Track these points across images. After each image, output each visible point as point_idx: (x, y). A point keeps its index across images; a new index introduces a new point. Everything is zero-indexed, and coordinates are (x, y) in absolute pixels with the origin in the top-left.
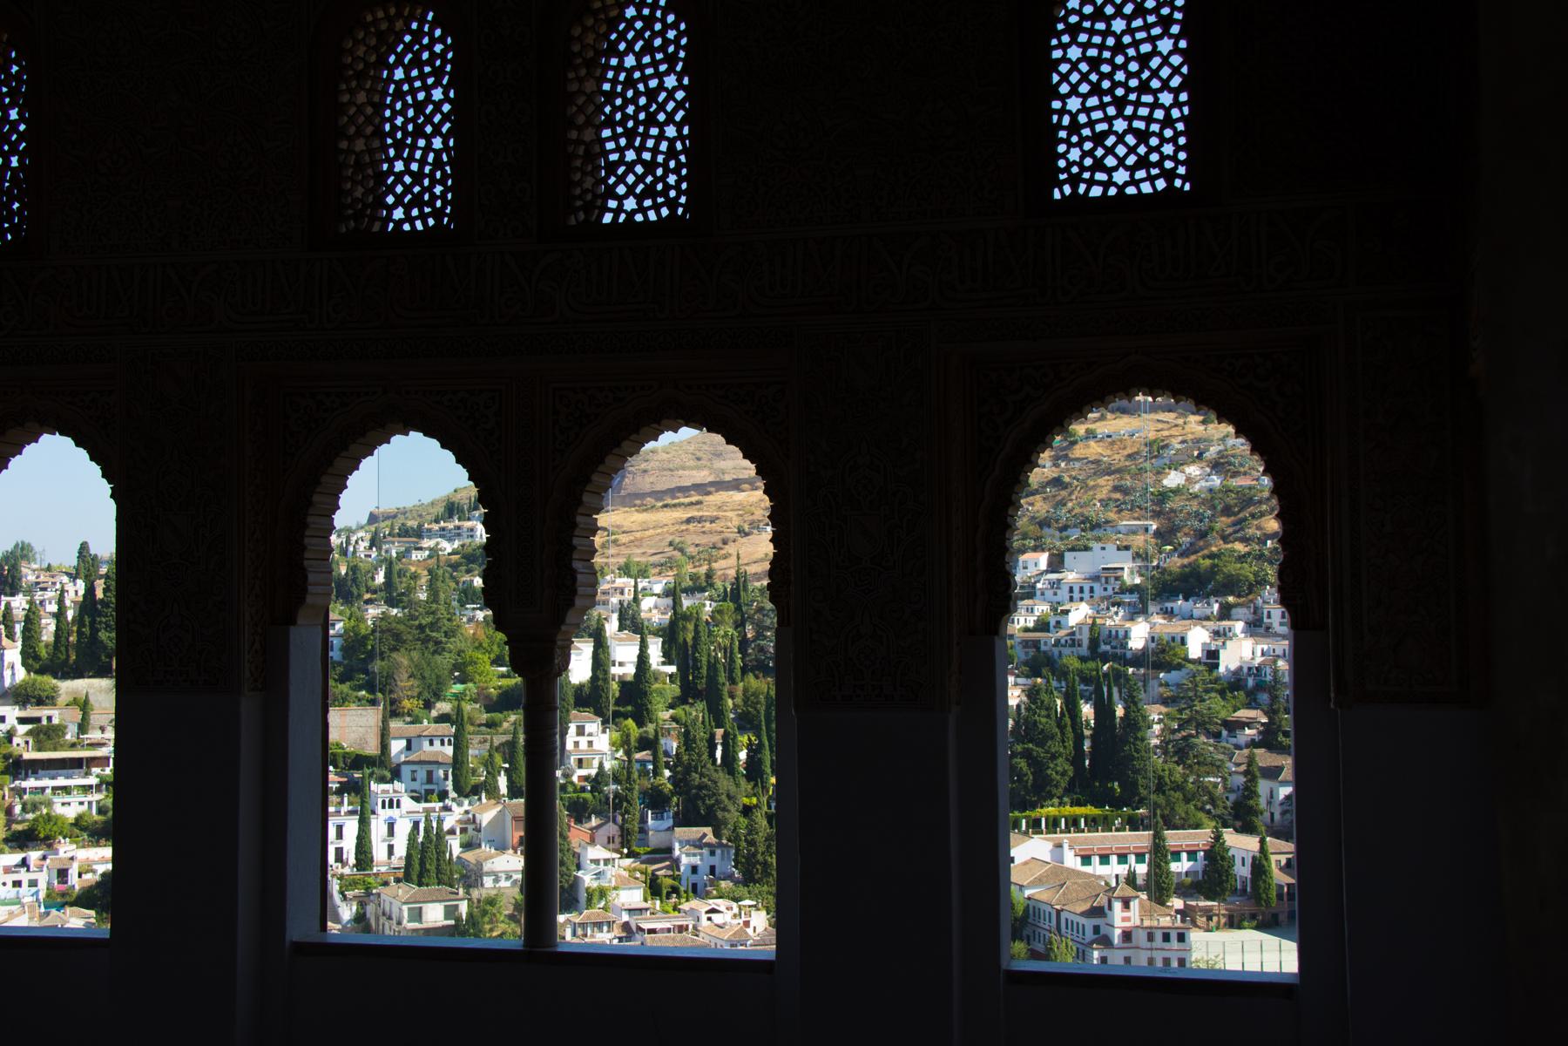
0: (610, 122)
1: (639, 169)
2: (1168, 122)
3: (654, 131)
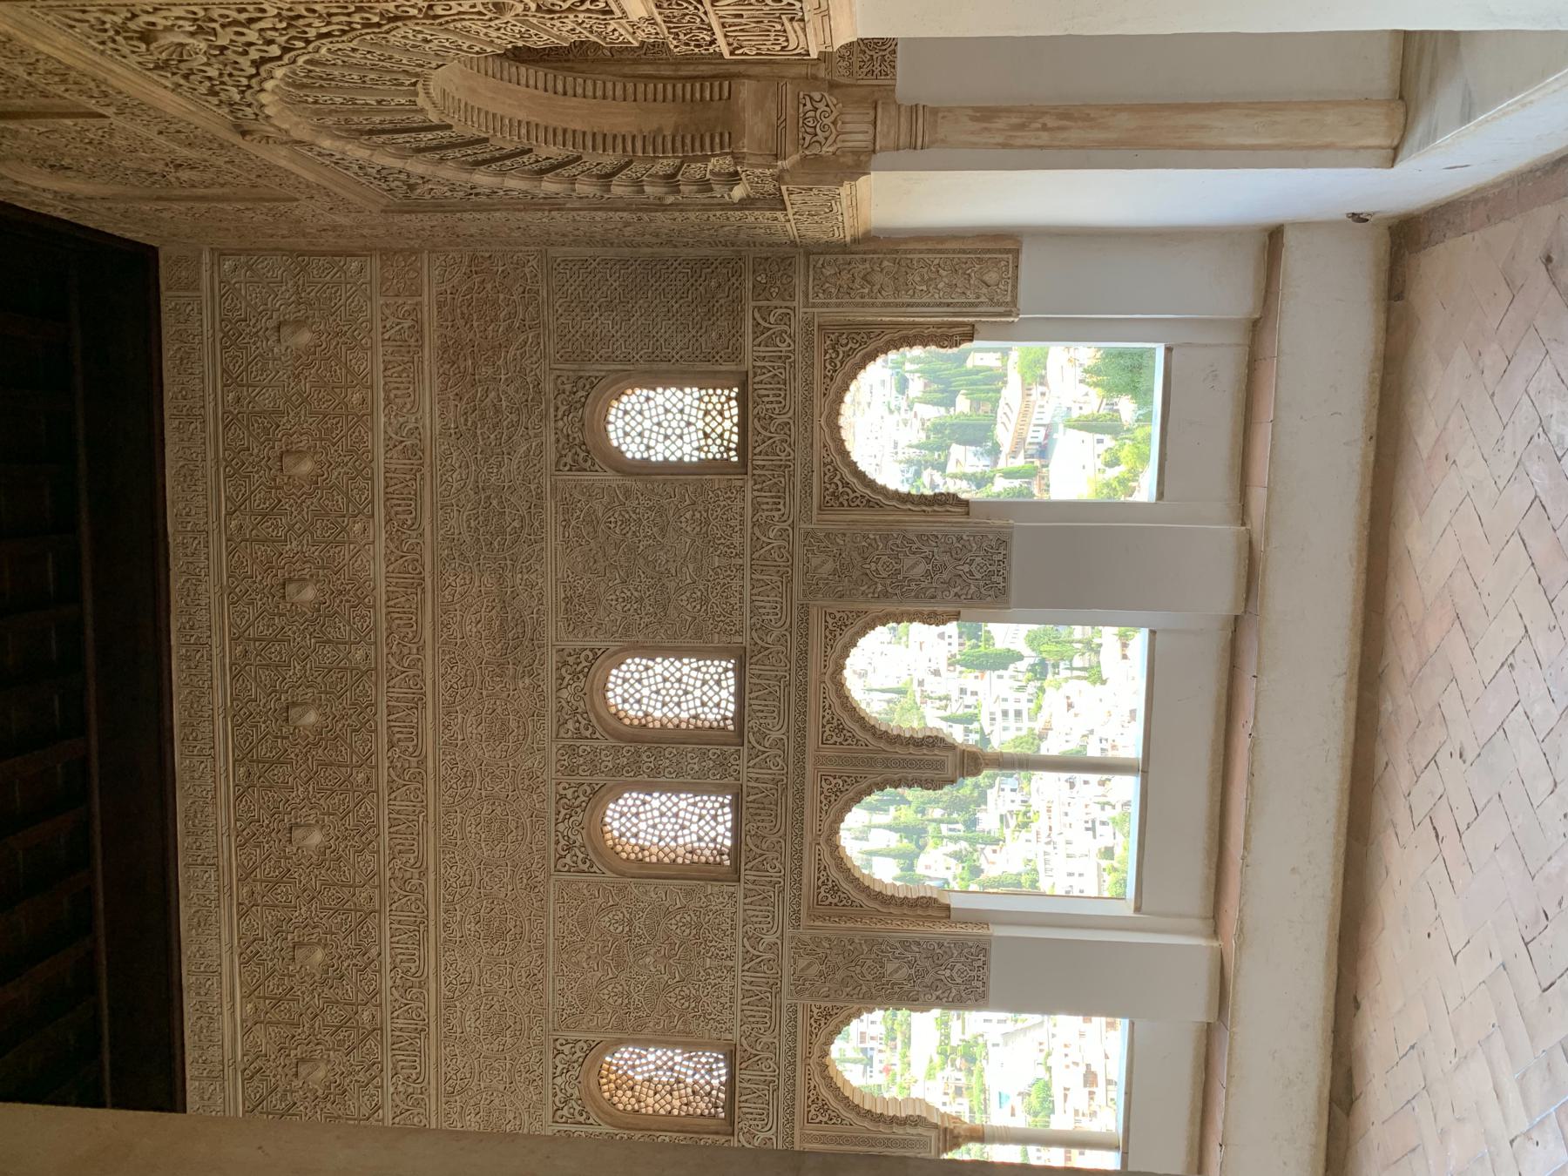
0: (675, 839)
1: (702, 823)
2: (698, 669)
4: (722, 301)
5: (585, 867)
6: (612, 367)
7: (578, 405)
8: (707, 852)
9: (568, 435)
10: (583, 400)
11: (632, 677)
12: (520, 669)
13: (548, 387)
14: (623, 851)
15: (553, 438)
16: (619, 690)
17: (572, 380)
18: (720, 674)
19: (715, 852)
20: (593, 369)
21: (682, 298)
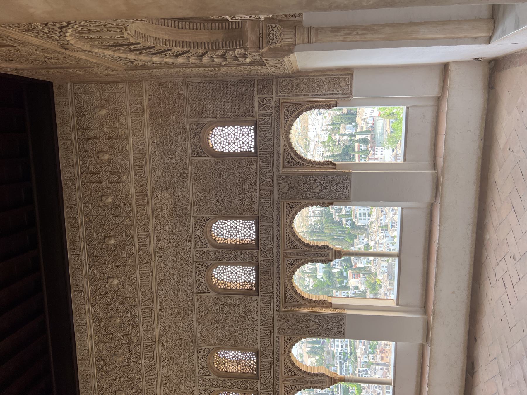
0: (236, 236)
1: (245, 230)
2: (241, 130)
3: (238, 227)
4: (247, 96)
5: (205, 246)
6: (209, 120)
7: (198, 134)
8: (247, 240)
9: (195, 144)
10: (200, 131)
11: (217, 134)
12: (182, 224)
13: (188, 127)
14: (218, 240)
15: (190, 145)
16: (213, 139)
17: (195, 125)
18: (248, 132)
19: (250, 240)
20: (203, 121)
21: (233, 95)
